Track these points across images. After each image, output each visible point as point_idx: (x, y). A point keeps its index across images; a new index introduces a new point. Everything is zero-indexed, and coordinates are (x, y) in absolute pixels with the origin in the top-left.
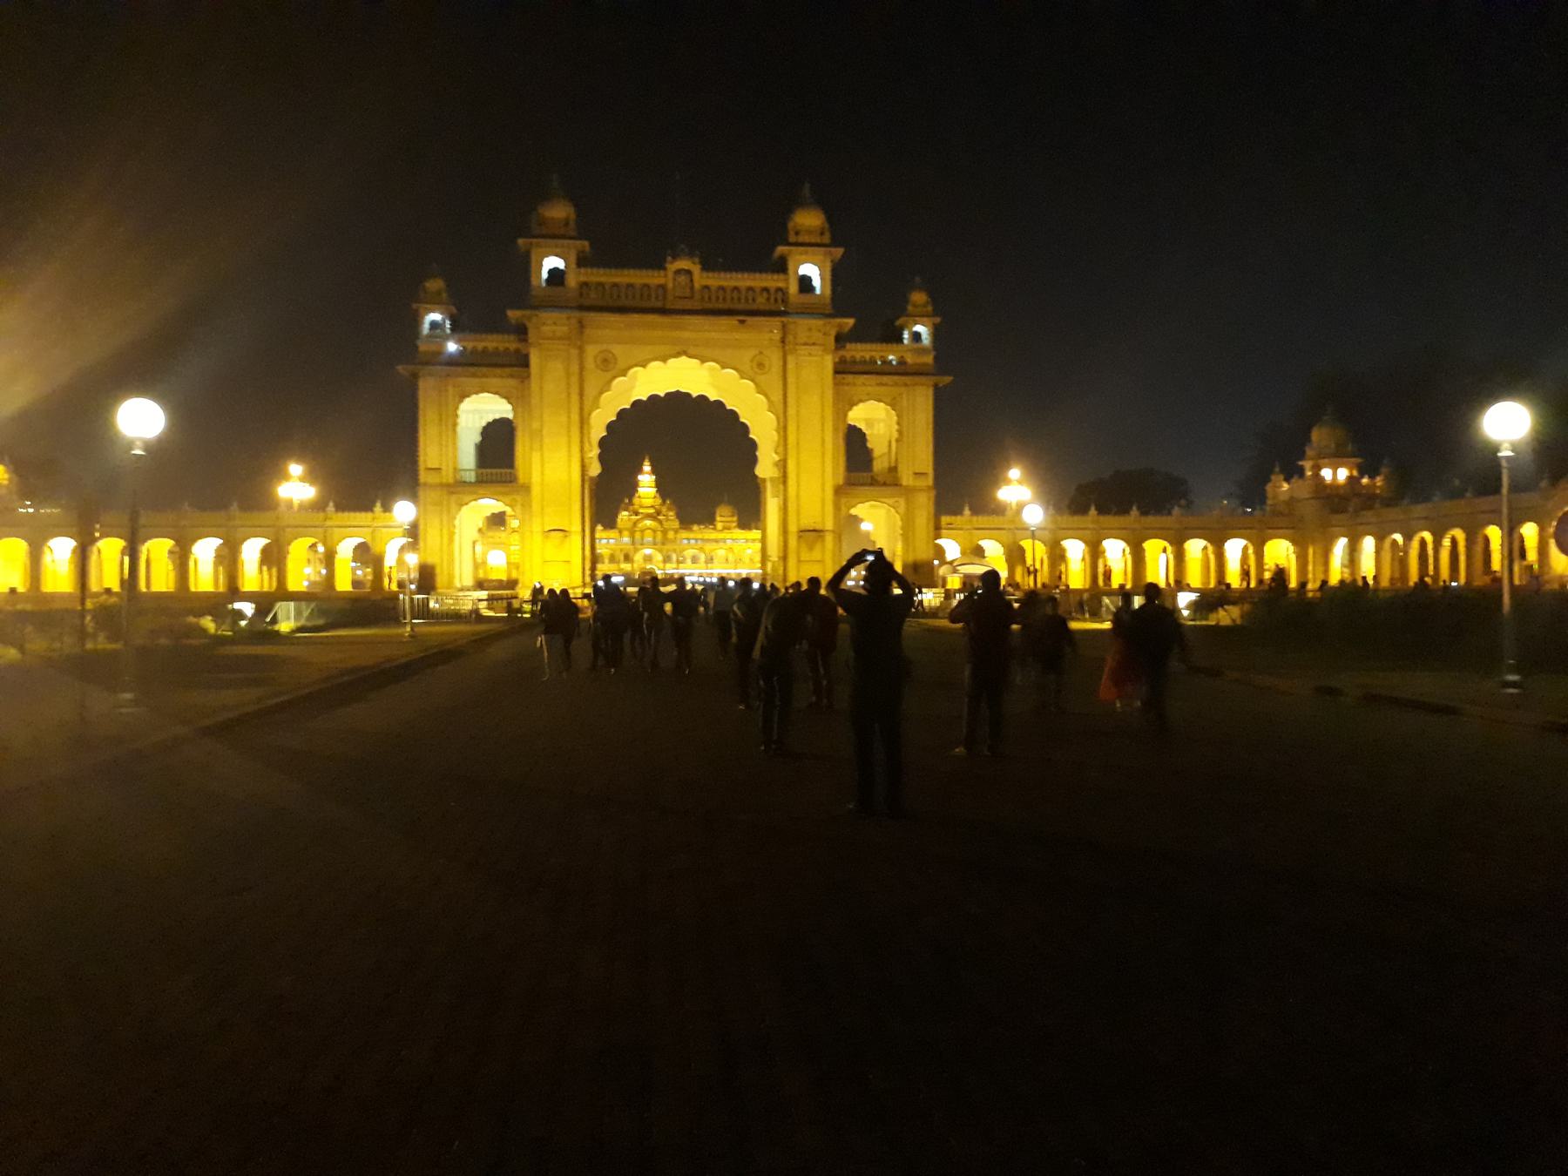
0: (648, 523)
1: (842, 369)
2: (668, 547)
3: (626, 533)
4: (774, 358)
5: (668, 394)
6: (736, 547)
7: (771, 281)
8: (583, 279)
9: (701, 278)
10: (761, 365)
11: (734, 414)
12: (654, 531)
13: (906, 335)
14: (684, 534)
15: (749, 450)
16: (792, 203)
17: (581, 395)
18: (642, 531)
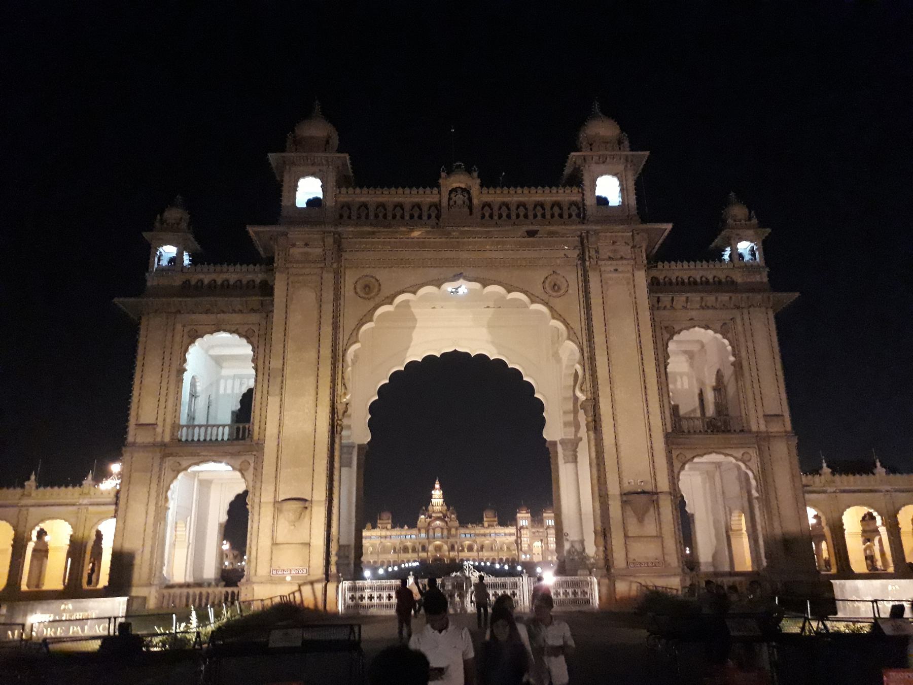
0: (438, 522)
1: (654, 285)
2: (452, 540)
3: (423, 531)
4: (572, 279)
5: (443, 355)
6: (498, 540)
7: (564, 195)
8: (343, 199)
9: (480, 195)
10: (555, 287)
11: (517, 374)
12: (442, 529)
13: (726, 257)
14: (462, 531)
15: (531, 410)
17: (336, 327)
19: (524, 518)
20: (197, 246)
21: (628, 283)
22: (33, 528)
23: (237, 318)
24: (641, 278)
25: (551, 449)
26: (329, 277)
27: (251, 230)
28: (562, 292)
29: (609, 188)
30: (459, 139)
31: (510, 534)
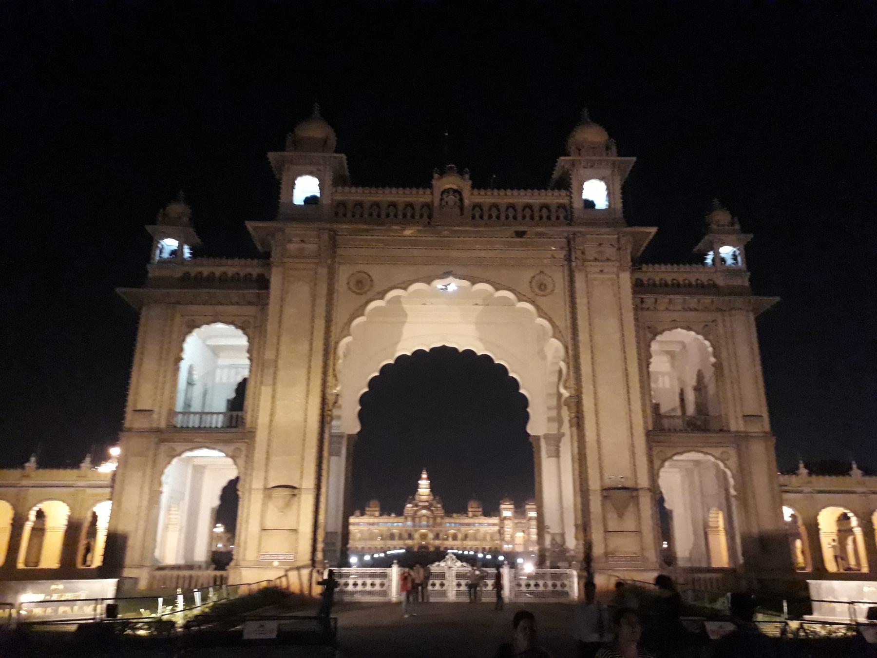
0: (424, 512)
1: (639, 287)
2: (438, 529)
3: (409, 519)
4: (558, 279)
7: (552, 198)
8: (339, 198)
9: (471, 197)
10: (542, 286)
11: (502, 369)
12: (428, 517)
13: (709, 260)
14: (447, 520)
15: (518, 406)
16: (571, 123)
17: (328, 321)
18: (420, 518)
19: (507, 510)
20: (197, 240)
21: (613, 284)
22: (30, 509)
23: (232, 309)
24: (626, 279)
25: (534, 445)
26: (323, 271)
27: (250, 225)
28: (548, 291)
29: (596, 192)
30: (451, 143)
31: (494, 525)
